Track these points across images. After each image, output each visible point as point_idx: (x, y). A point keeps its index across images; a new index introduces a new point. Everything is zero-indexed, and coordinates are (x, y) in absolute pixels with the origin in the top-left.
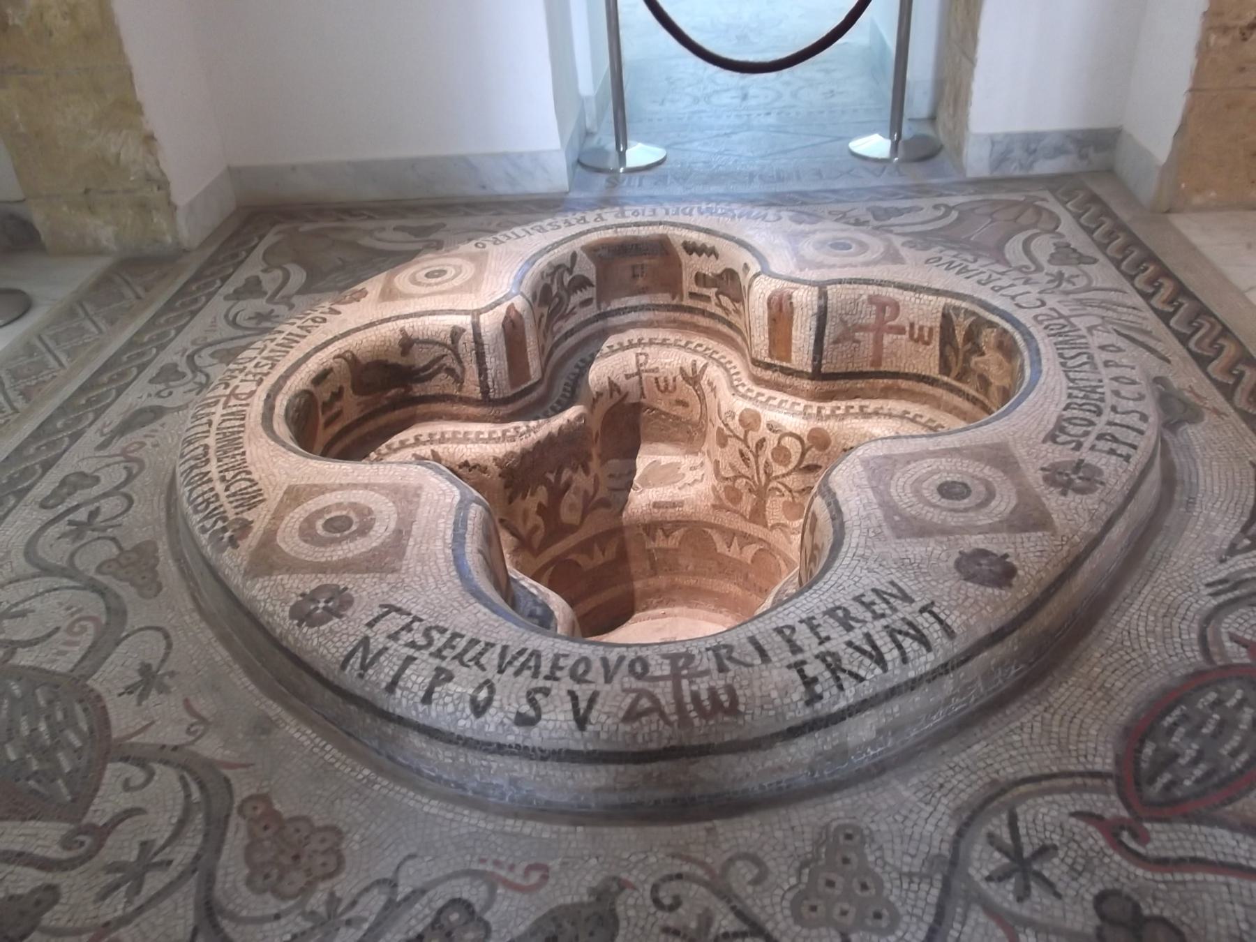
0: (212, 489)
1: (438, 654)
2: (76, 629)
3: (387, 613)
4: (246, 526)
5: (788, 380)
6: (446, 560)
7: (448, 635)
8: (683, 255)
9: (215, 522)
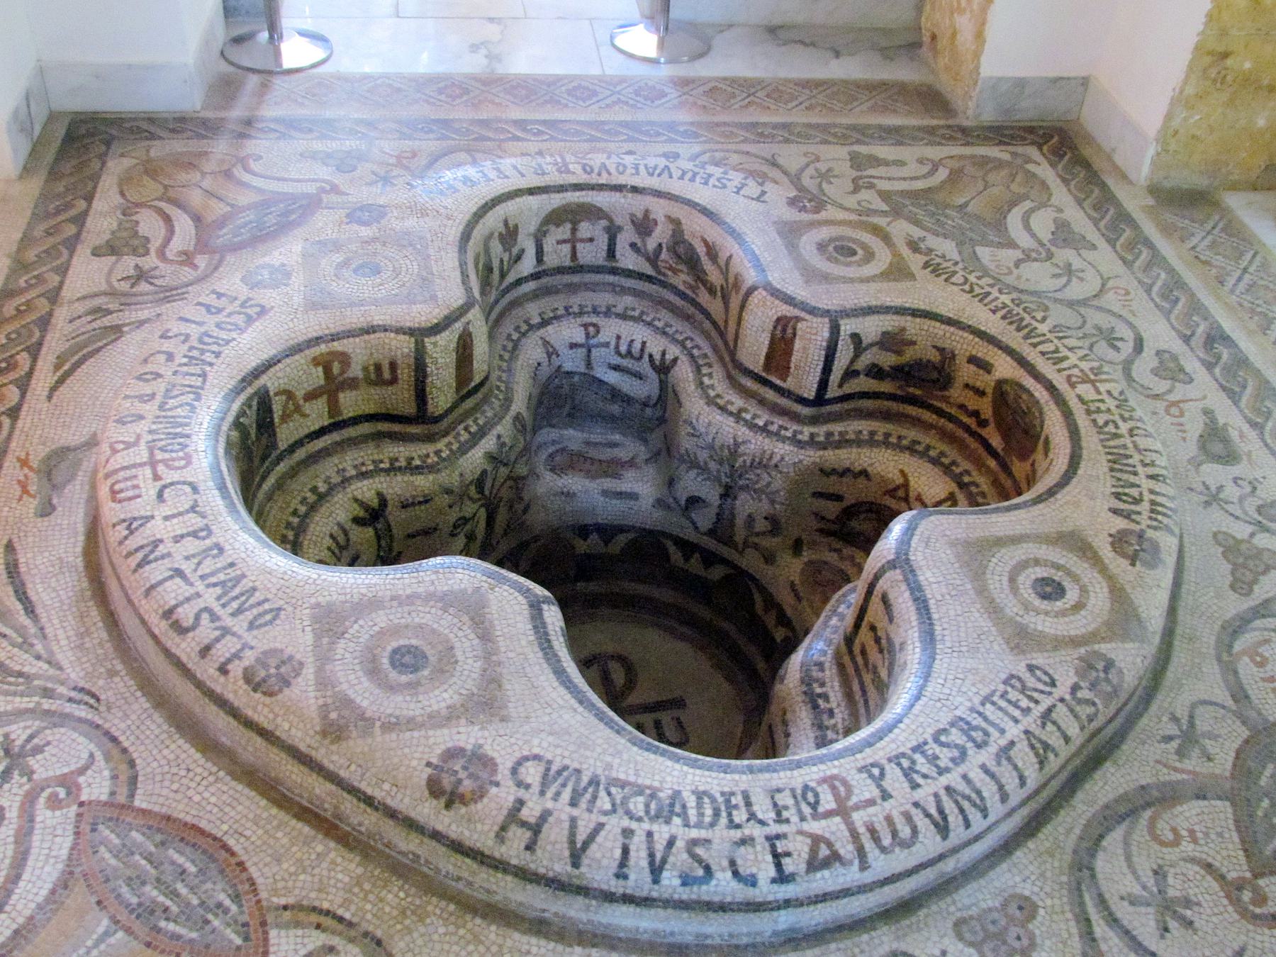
1: (710, 176)
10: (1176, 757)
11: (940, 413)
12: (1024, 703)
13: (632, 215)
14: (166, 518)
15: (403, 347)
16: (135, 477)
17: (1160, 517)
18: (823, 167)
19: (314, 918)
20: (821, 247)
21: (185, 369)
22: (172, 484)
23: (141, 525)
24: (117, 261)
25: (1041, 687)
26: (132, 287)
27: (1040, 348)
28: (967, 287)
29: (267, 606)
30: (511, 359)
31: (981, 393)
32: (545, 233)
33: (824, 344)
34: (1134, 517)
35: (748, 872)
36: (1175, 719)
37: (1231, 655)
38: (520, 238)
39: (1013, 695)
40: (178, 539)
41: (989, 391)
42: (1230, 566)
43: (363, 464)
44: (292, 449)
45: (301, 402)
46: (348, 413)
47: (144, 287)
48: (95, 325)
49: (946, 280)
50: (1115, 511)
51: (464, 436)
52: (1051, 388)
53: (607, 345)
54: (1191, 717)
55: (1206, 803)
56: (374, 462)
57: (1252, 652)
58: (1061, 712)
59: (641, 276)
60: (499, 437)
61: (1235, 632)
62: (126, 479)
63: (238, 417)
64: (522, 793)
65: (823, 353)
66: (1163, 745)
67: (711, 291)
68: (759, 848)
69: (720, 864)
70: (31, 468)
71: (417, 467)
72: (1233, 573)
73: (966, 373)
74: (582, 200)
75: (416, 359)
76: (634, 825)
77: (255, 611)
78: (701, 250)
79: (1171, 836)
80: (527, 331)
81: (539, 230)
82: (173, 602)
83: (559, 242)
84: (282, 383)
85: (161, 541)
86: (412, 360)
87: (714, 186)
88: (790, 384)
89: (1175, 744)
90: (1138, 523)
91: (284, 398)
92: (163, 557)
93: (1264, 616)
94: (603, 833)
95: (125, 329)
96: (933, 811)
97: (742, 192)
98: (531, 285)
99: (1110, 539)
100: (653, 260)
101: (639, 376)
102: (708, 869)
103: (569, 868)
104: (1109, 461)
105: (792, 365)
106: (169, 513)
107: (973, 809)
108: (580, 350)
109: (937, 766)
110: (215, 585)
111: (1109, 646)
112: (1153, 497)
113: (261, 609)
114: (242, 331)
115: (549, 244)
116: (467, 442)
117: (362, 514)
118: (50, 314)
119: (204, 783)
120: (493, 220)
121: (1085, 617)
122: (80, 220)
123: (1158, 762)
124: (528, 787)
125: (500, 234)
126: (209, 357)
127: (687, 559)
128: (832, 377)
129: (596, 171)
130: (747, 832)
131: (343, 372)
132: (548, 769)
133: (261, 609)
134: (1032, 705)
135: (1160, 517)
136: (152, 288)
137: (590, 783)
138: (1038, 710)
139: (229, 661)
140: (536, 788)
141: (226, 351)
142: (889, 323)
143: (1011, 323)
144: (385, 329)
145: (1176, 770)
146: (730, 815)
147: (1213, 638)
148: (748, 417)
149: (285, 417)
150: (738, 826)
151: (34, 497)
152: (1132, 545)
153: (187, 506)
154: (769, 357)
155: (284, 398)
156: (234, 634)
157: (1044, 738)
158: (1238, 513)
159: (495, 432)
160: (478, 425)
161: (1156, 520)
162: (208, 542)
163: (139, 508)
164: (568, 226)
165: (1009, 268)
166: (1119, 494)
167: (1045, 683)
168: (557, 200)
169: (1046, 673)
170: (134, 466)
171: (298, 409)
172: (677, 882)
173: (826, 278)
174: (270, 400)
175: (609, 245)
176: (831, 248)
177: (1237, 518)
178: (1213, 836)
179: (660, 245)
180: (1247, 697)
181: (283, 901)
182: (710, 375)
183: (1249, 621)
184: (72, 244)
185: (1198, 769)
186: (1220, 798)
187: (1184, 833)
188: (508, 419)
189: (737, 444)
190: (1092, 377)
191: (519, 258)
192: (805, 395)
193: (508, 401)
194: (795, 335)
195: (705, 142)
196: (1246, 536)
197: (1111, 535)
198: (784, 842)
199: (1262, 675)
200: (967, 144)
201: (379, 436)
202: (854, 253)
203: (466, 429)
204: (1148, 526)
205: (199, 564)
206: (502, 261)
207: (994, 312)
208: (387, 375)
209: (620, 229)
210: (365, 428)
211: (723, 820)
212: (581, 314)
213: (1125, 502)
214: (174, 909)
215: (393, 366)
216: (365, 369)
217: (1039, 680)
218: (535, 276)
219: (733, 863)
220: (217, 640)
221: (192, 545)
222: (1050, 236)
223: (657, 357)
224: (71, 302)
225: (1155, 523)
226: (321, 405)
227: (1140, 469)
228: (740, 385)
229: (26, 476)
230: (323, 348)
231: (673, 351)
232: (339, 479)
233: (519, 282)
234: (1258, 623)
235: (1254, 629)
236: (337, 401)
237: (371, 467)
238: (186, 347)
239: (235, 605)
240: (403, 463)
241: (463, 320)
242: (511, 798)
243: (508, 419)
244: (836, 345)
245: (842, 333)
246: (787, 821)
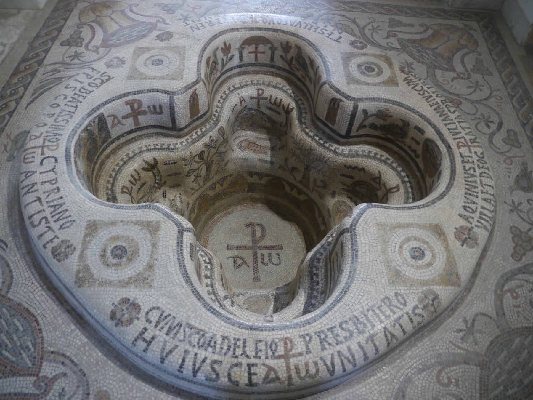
1: (318, 27)
3: (338, 40)
6: (327, 57)
7: (317, 32)
10: (460, 341)
11: (401, 148)
13: (281, 43)
14: (41, 173)
15: (164, 99)
16: (34, 152)
17: (483, 221)
18: (375, 25)
19: (62, 359)
20: (359, 66)
21: (69, 103)
22: (48, 157)
23: (31, 175)
24: (68, 49)
25: (399, 305)
26: (71, 60)
27: (449, 126)
28: (422, 92)
29: (69, 219)
30: (223, 102)
31: (418, 143)
32: (243, 48)
33: (350, 113)
34: (470, 220)
35: (236, 379)
36: (465, 321)
38: (232, 50)
39: (385, 308)
40: (43, 183)
41: (422, 143)
42: (514, 245)
43: (150, 145)
44: (118, 138)
45: (121, 119)
46: (143, 124)
47: (76, 61)
48: (52, 77)
49: (412, 88)
50: (460, 216)
51: (195, 136)
52: (449, 147)
53: (266, 99)
54: (474, 321)
55: (468, 366)
56: (154, 145)
59: (284, 70)
60: (211, 137)
61: (507, 279)
62: (31, 153)
63: (87, 127)
64: (147, 325)
65: (350, 117)
66: (456, 334)
67: (310, 80)
68: (243, 369)
69: (223, 374)
70: (10, 139)
71: (172, 149)
72: (514, 249)
73: (412, 133)
74: (260, 35)
75: (170, 105)
76: (190, 349)
77: (64, 221)
78: (308, 62)
79: (446, 381)
80: (233, 90)
81: (241, 47)
82: (33, 213)
83: (250, 53)
84: (111, 112)
85: (36, 183)
86: (169, 105)
87: (319, 33)
88: (335, 127)
89: (461, 334)
90: (471, 223)
91: (112, 118)
92: (35, 191)
93: (524, 273)
94: (176, 351)
95: (63, 79)
96: (329, 363)
97: (330, 37)
98: (238, 70)
99: (455, 230)
100: (289, 63)
101: (278, 113)
102: (217, 375)
103: (160, 363)
104: (466, 189)
105: (337, 120)
106: (43, 171)
107: (348, 364)
108: (255, 100)
109: (337, 340)
110: (52, 206)
111: (438, 287)
112: (482, 210)
113: (66, 220)
114: (97, 87)
115: (245, 53)
116: (195, 139)
117: (146, 166)
118: (37, 71)
119: (37, 290)
120: (218, 42)
121: (430, 271)
122: (60, 30)
123: (451, 342)
124: (150, 322)
125: (222, 48)
126: (81, 99)
127: (292, 190)
128: (353, 127)
129: (268, 22)
130: (240, 360)
131: (139, 108)
132: (162, 315)
133: (66, 220)
134: (391, 314)
135: (483, 221)
136: (79, 62)
137: (178, 324)
139: (46, 244)
140: (154, 324)
141: (89, 96)
142: (381, 106)
143: (437, 113)
144: (158, 91)
145: (459, 348)
146: (234, 350)
147: (496, 281)
148: (317, 139)
149: (113, 126)
150: (236, 357)
151: (8, 152)
152: (465, 234)
153: (51, 168)
154: (328, 114)
155: (112, 118)
156: (53, 231)
157: (393, 332)
158: (525, 217)
159: (209, 135)
160: (202, 131)
161: (480, 222)
162: (55, 186)
163: (32, 167)
164: (254, 46)
165: (448, 81)
166: (466, 206)
167: (401, 303)
168: (249, 34)
169: (403, 298)
170: (35, 147)
171: (119, 122)
172: (203, 378)
173: (357, 82)
174: (105, 119)
175: (271, 55)
176: (363, 68)
177: (524, 220)
178: (467, 385)
179: (292, 58)
180: (504, 314)
181: (52, 349)
182: (305, 118)
183: (517, 274)
184: (53, 40)
185: (469, 349)
186: (476, 365)
187: (453, 381)
188: (216, 129)
189: (310, 149)
190: (470, 144)
191: (231, 58)
192: (341, 133)
193: (218, 121)
194: (338, 107)
195: (327, 9)
196: (526, 231)
197: (456, 228)
198: (255, 368)
199: (514, 303)
200: (445, 18)
201: (158, 134)
202: (373, 70)
203: (196, 133)
204: (476, 226)
205: (48, 196)
206: (223, 60)
207: (431, 106)
208: (158, 110)
209: (276, 49)
210: (152, 130)
211: (231, 353)
212: (257, 84)
213: (468, 211)
214: (10, 346)
215: (160, 107)
216: (149, 107)
217: (398, 301)
218: (239, 66)
219: (229, 374)
220: (46, 232)
221: (48, 187)
222: (472, 67)
223: (286, 106)
224: (46, 66)
225: (479, 224)
226: (131, 120)
227: (480, 194)
228: (316, 124)
229: (7, 142)
230: (130, 97)
231: (293, 105)
232: (139, 151)
233: (231, 69)
234: (520, 276)
235: (517, 279)
236: (138, 120)
237: (153, 147)
238: (73, 93)
239: (57, 217)
240: (166, 146)
241: (194, 88)
242: (142, 327)
243: (216, 129)
244: (356, 114)
245: (359, 109)
246: (260, 357)
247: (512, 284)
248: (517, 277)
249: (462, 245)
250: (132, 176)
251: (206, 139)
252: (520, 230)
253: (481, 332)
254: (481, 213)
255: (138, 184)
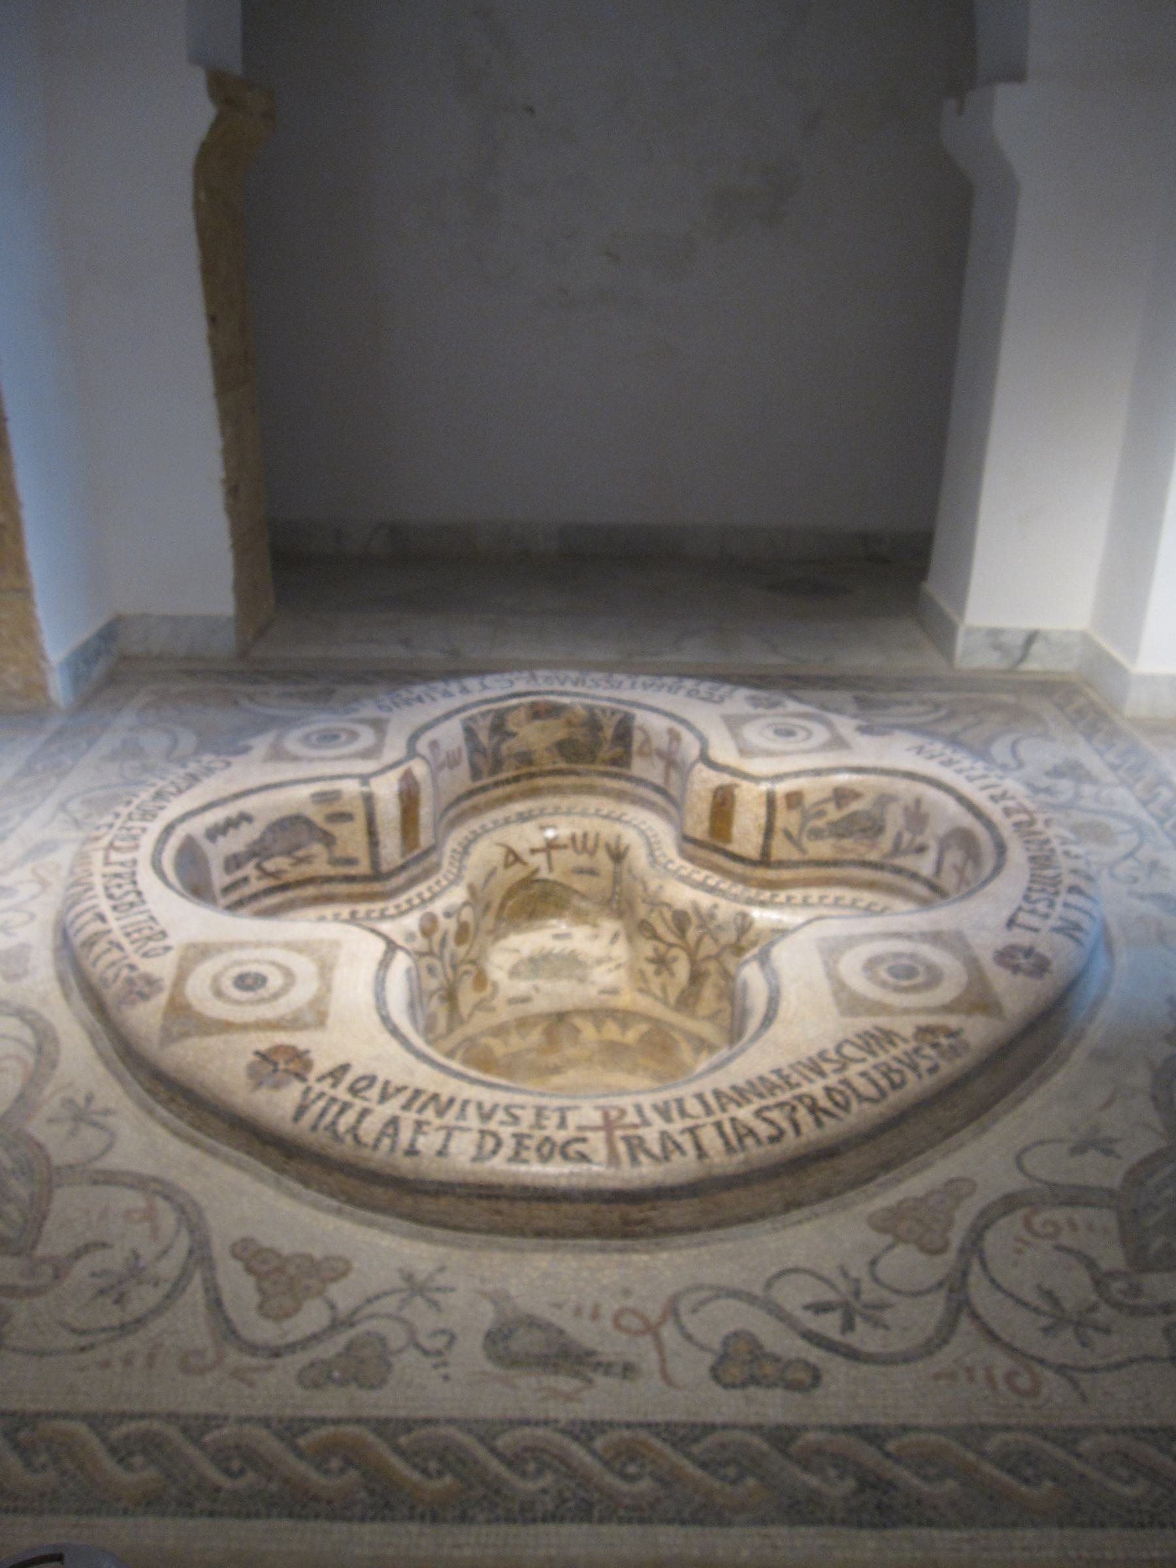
0: (863, 1074)
2: (1050, 1229)
4: (924, 1032)
5: (426, 864)
8: (207, 846)
9: (924, 1057)
12: (136, 936)
36: (107, 1112)
37: (155, 1192)
38: (928, 831)
39: (147, 932)
50: (344, 1068)
57: (150, 1215)
58: (115, 954)
60: (716, 906)
93: (191, 1252)
135: (321, 1104)
138: (125, 942)
152: (287, 1062)
183: (192, 1232)
191: (921, 849)
204: (308, 1090)
206: (899, 835)
225: (312, 1096)
227: (411, 1116)
233: (914, 876)
234: (183, 1242)
235: (177, 1232)
241: (737, 780)
247: (168, 1218)
248: (184, 1233)
249: (257, 1053)
250: (585, 835)
251: (705, 900)
252: (333, 1280)
253: (73, 1133)
254: (345, 1107)
255: (583, 860)
